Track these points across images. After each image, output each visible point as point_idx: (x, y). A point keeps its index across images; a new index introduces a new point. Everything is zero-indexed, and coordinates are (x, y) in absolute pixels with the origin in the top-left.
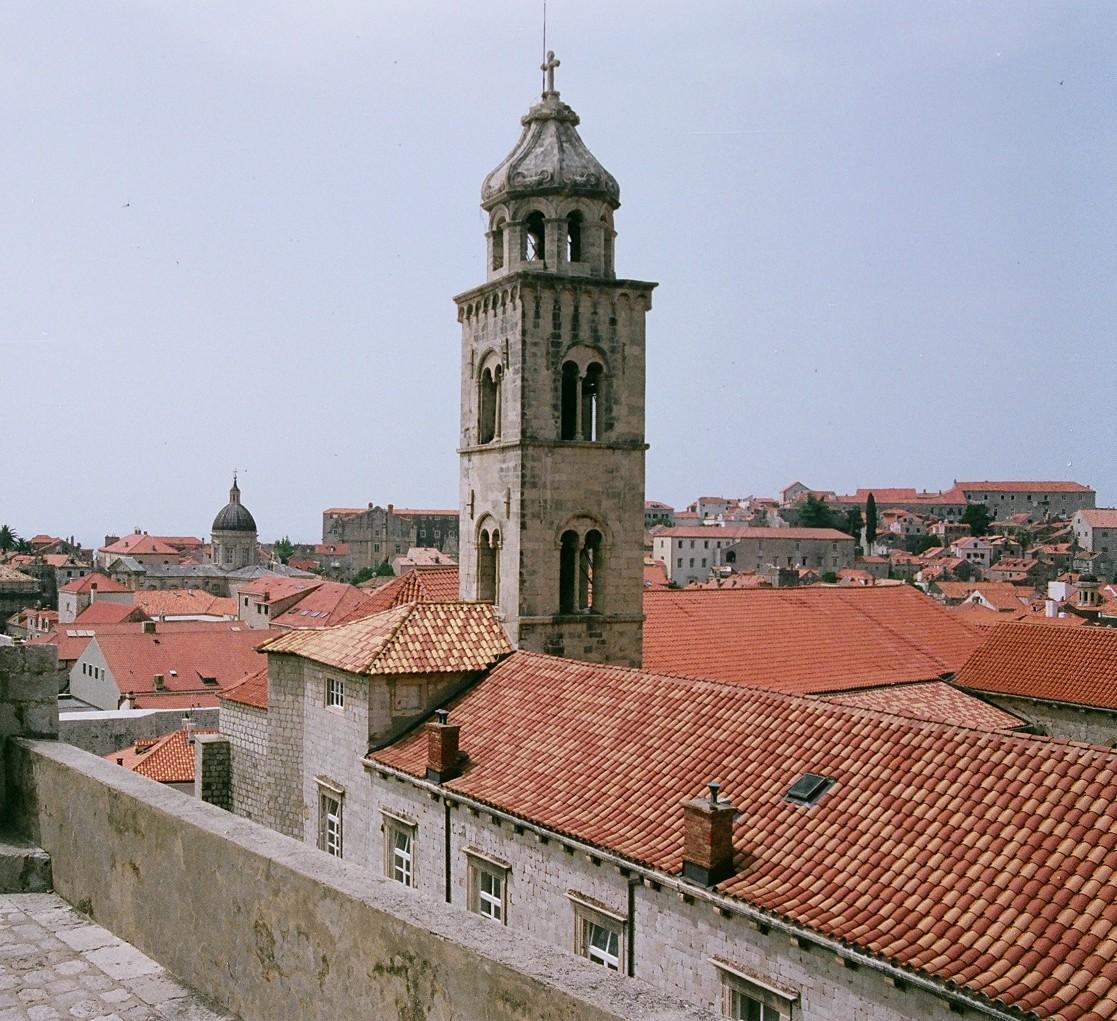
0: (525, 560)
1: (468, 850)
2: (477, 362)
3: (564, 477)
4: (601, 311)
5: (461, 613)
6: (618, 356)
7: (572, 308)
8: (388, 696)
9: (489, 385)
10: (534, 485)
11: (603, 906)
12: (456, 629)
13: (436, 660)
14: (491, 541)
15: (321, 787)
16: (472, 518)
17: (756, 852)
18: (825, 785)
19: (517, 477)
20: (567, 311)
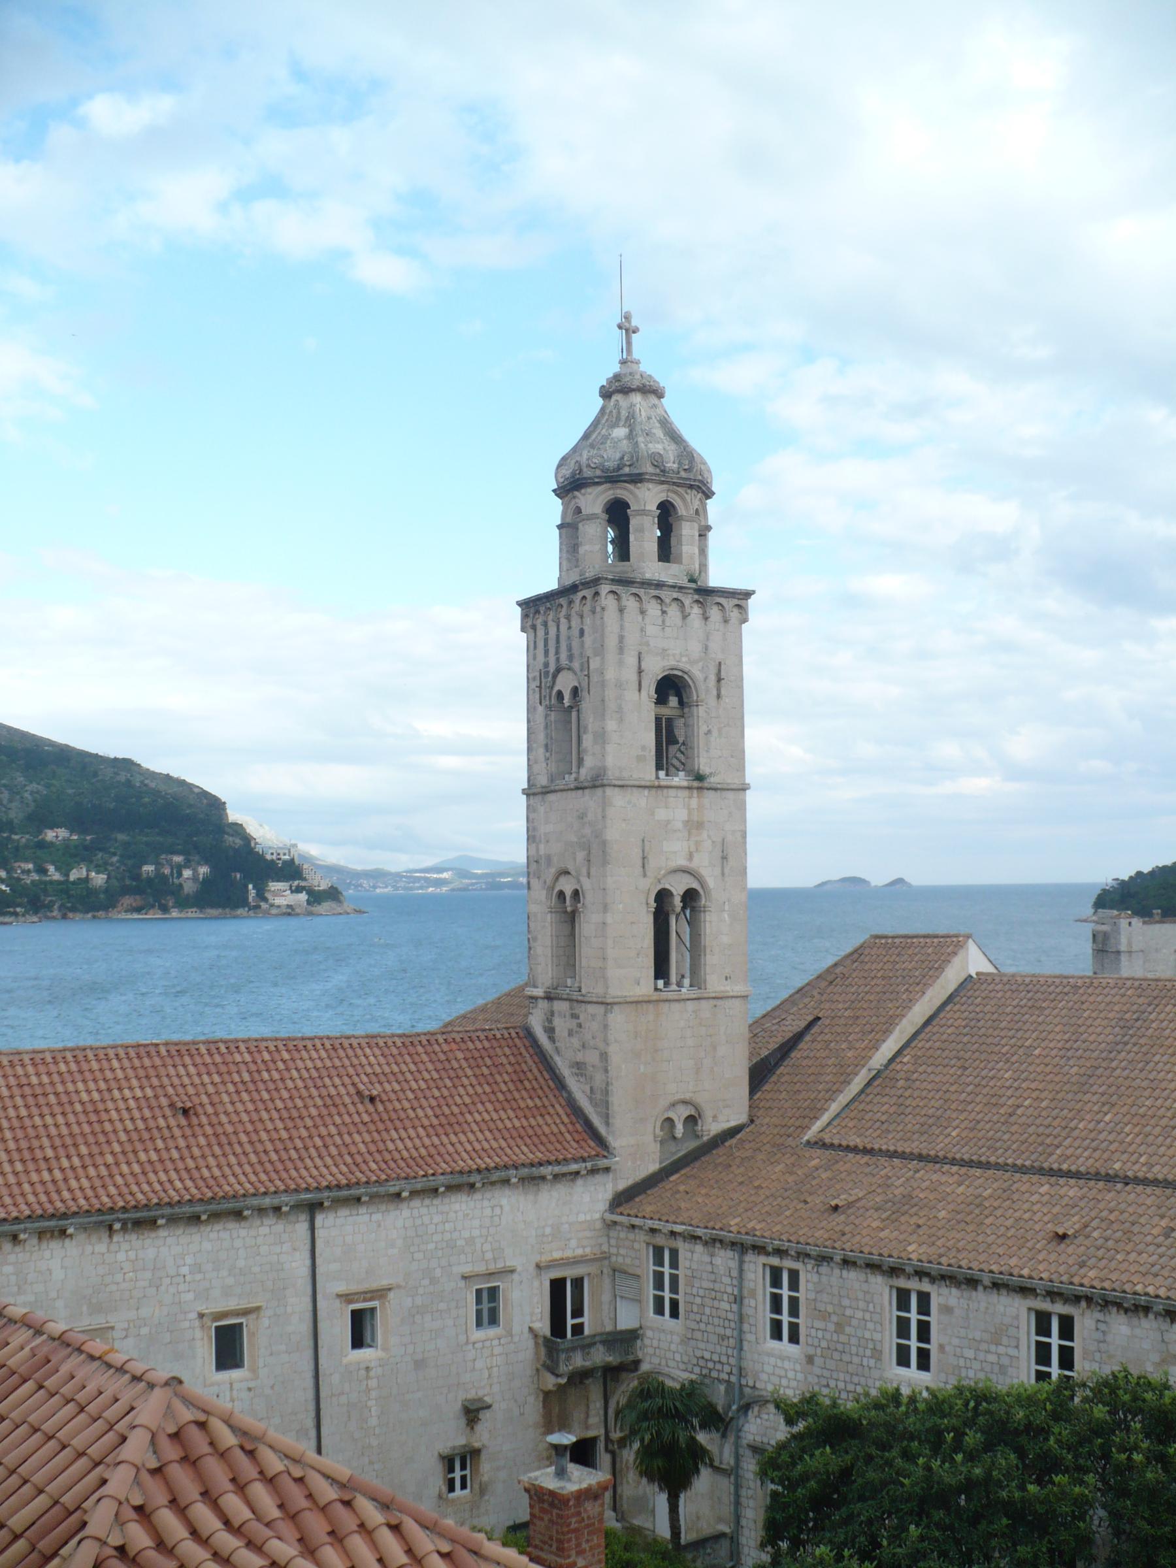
4: (573, 624)
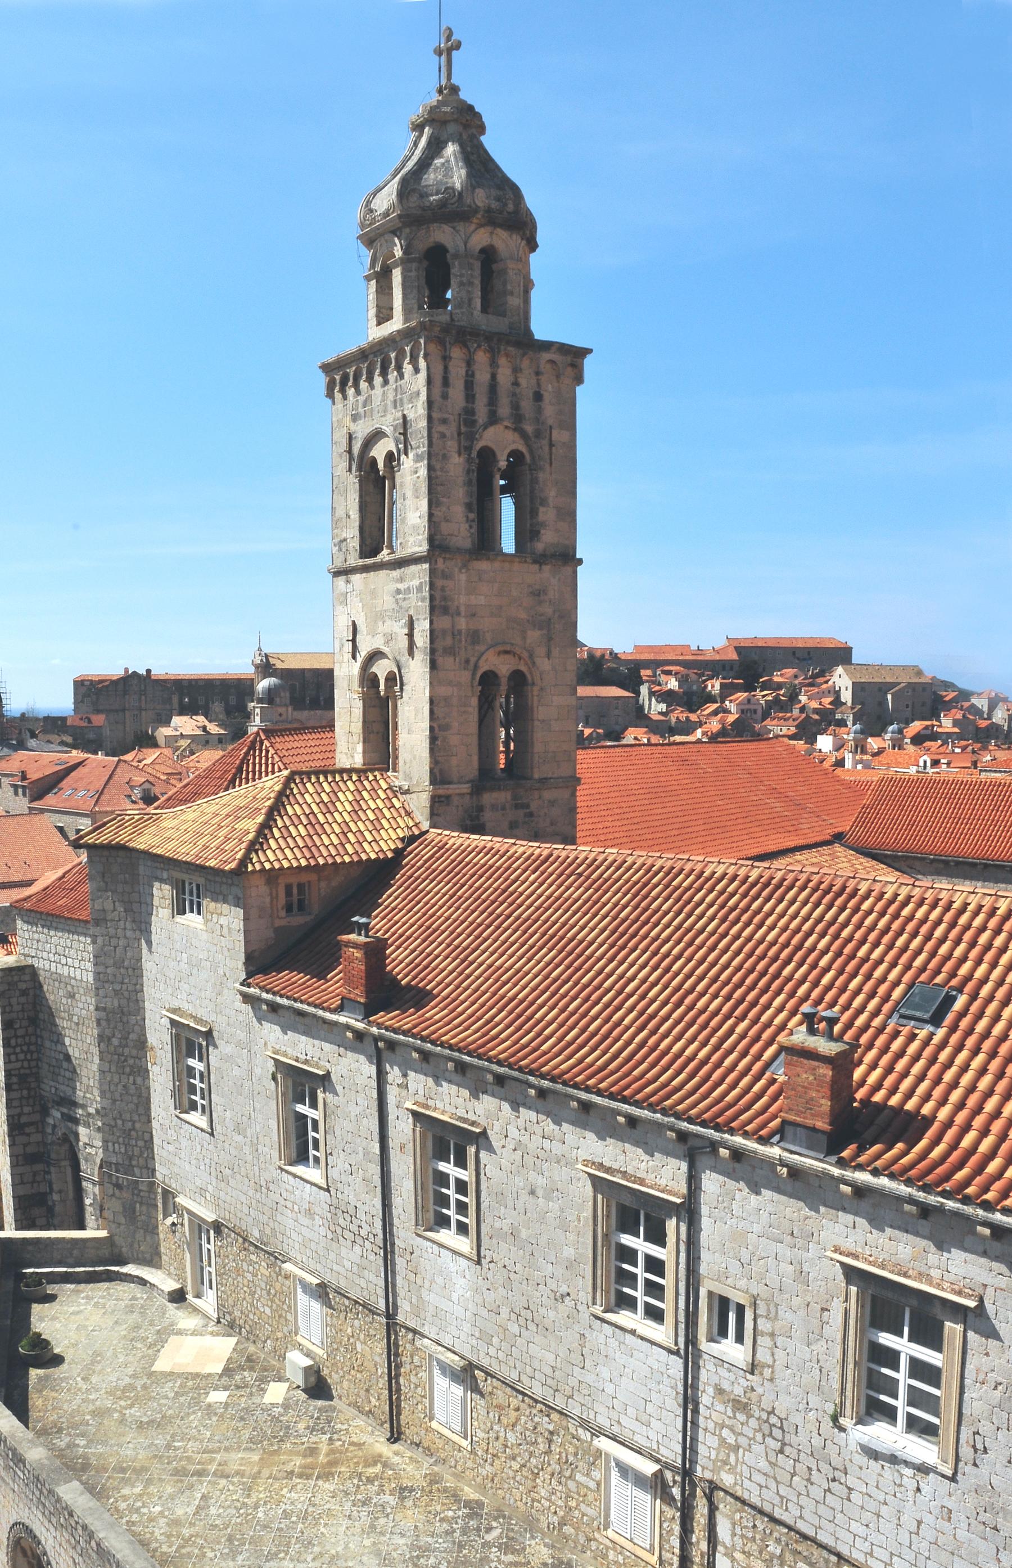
0: (435, 709)
1: (415, 1108)
2: (356, 450)
3: (482, 600)
4: (523, 382)
5: (349, 783)
6: (545, 442)
7: (488, 376)
8: (268, 900)
9: (375, 483)
10: (445, 611)
11: (642, 1182)
12: (346, 804)
13: (330, 848)
14: (382, 687)
15: (173, 1022)
16: (354, 657)
17: (926, 1110)
18: (949, 1001)
19: (423, 600)
20: (483, 377)
